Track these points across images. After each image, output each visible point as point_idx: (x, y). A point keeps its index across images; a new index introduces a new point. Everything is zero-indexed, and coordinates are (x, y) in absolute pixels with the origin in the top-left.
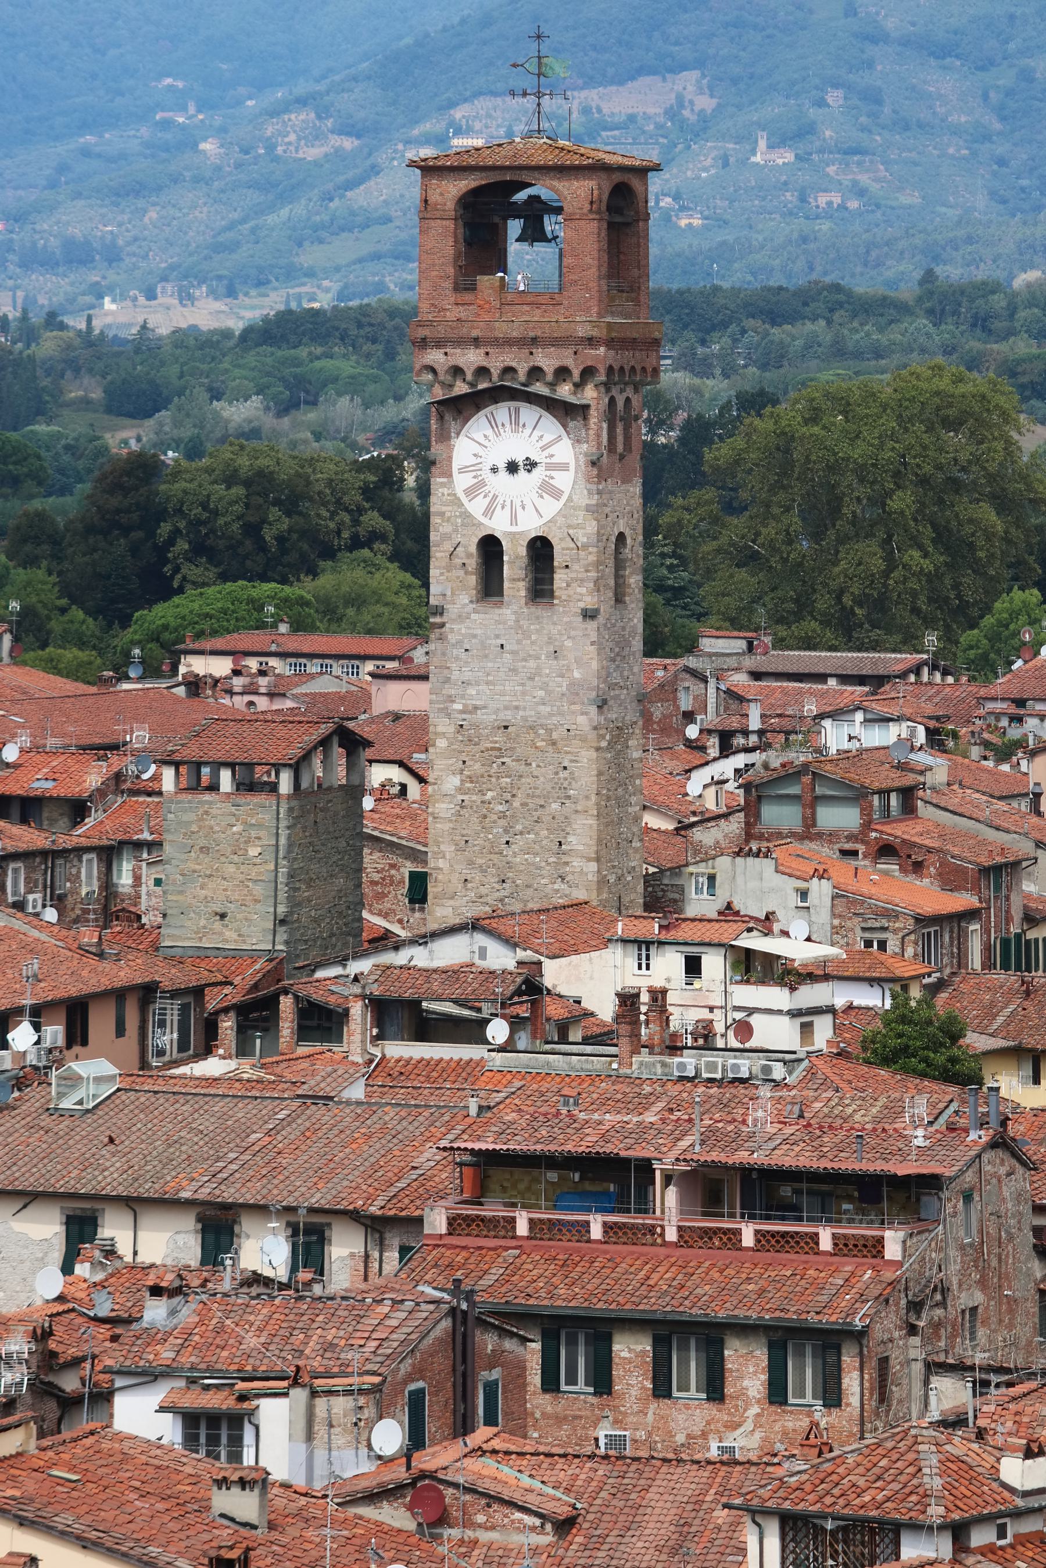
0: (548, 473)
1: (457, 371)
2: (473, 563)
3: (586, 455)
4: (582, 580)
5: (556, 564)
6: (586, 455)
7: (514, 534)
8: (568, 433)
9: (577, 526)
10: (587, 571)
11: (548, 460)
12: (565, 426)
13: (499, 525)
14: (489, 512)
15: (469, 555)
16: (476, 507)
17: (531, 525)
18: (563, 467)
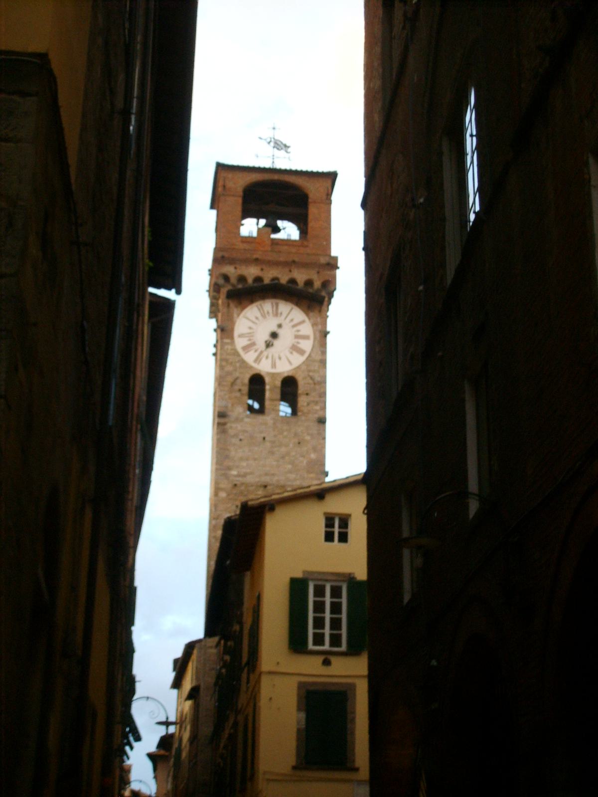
1: (242, 279)
3: (320, 332)
8: (309, 319)
9: (314, 371)
11: (296, 333)
12: (307, 315)
13: (264, 367)
14: (258, 360)
15: (243, 385)
16: (249, 357)
17: (284, 368)
18: (306, 337)
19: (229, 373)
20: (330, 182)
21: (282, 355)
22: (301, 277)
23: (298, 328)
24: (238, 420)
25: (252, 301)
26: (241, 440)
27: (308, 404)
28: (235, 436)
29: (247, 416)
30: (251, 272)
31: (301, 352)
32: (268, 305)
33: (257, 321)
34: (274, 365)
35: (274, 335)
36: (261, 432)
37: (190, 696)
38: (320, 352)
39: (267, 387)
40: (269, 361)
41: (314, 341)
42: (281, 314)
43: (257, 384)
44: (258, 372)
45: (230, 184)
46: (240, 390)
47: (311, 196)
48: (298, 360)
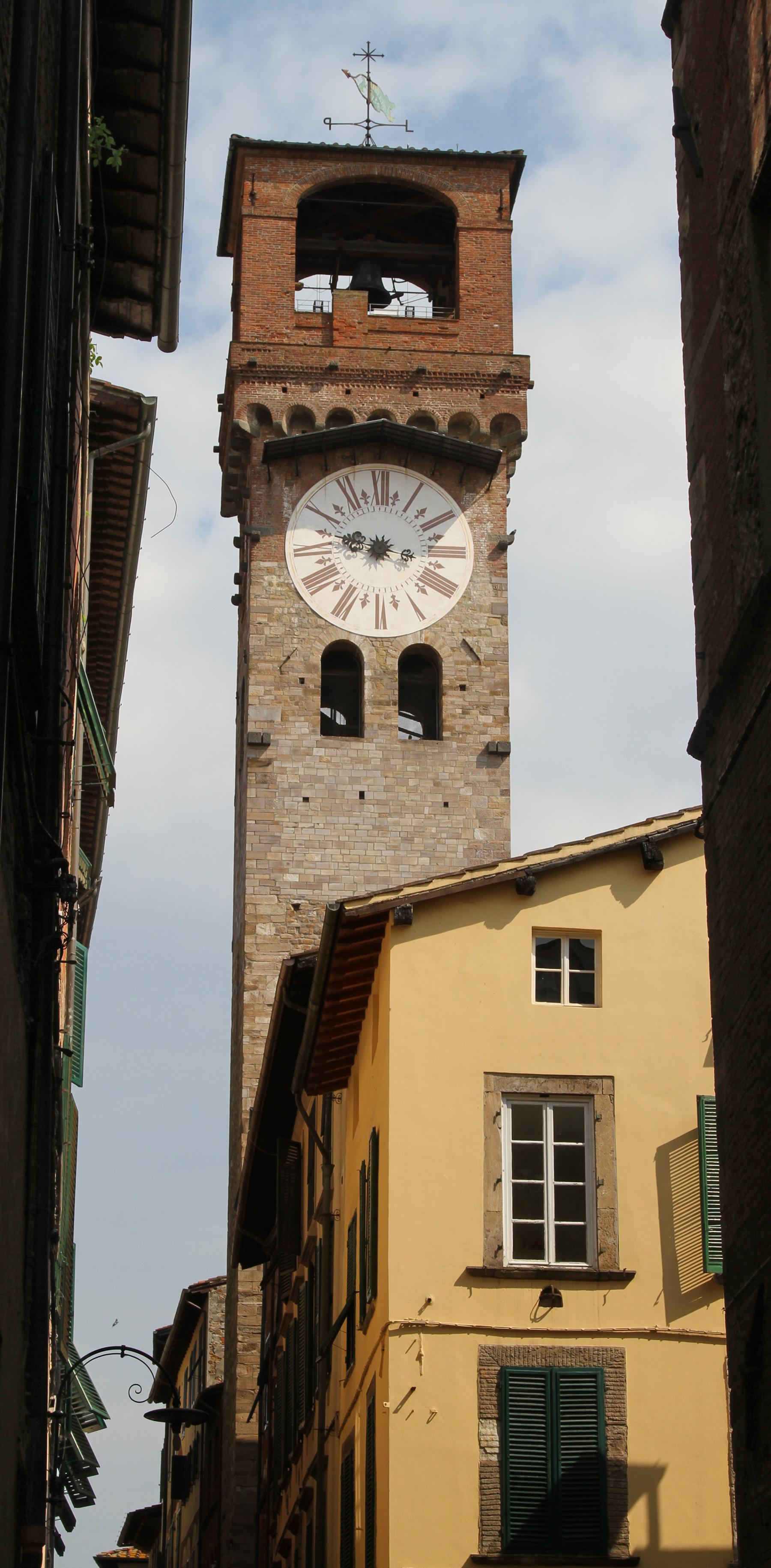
5: (445, 682)
13: (358, 626)
15: (310, 668)
16: (323, 602)
21: (400, 596)
32: (362, 478)
41: (476, 560)
42: (396, 495)
44: (344, 637)
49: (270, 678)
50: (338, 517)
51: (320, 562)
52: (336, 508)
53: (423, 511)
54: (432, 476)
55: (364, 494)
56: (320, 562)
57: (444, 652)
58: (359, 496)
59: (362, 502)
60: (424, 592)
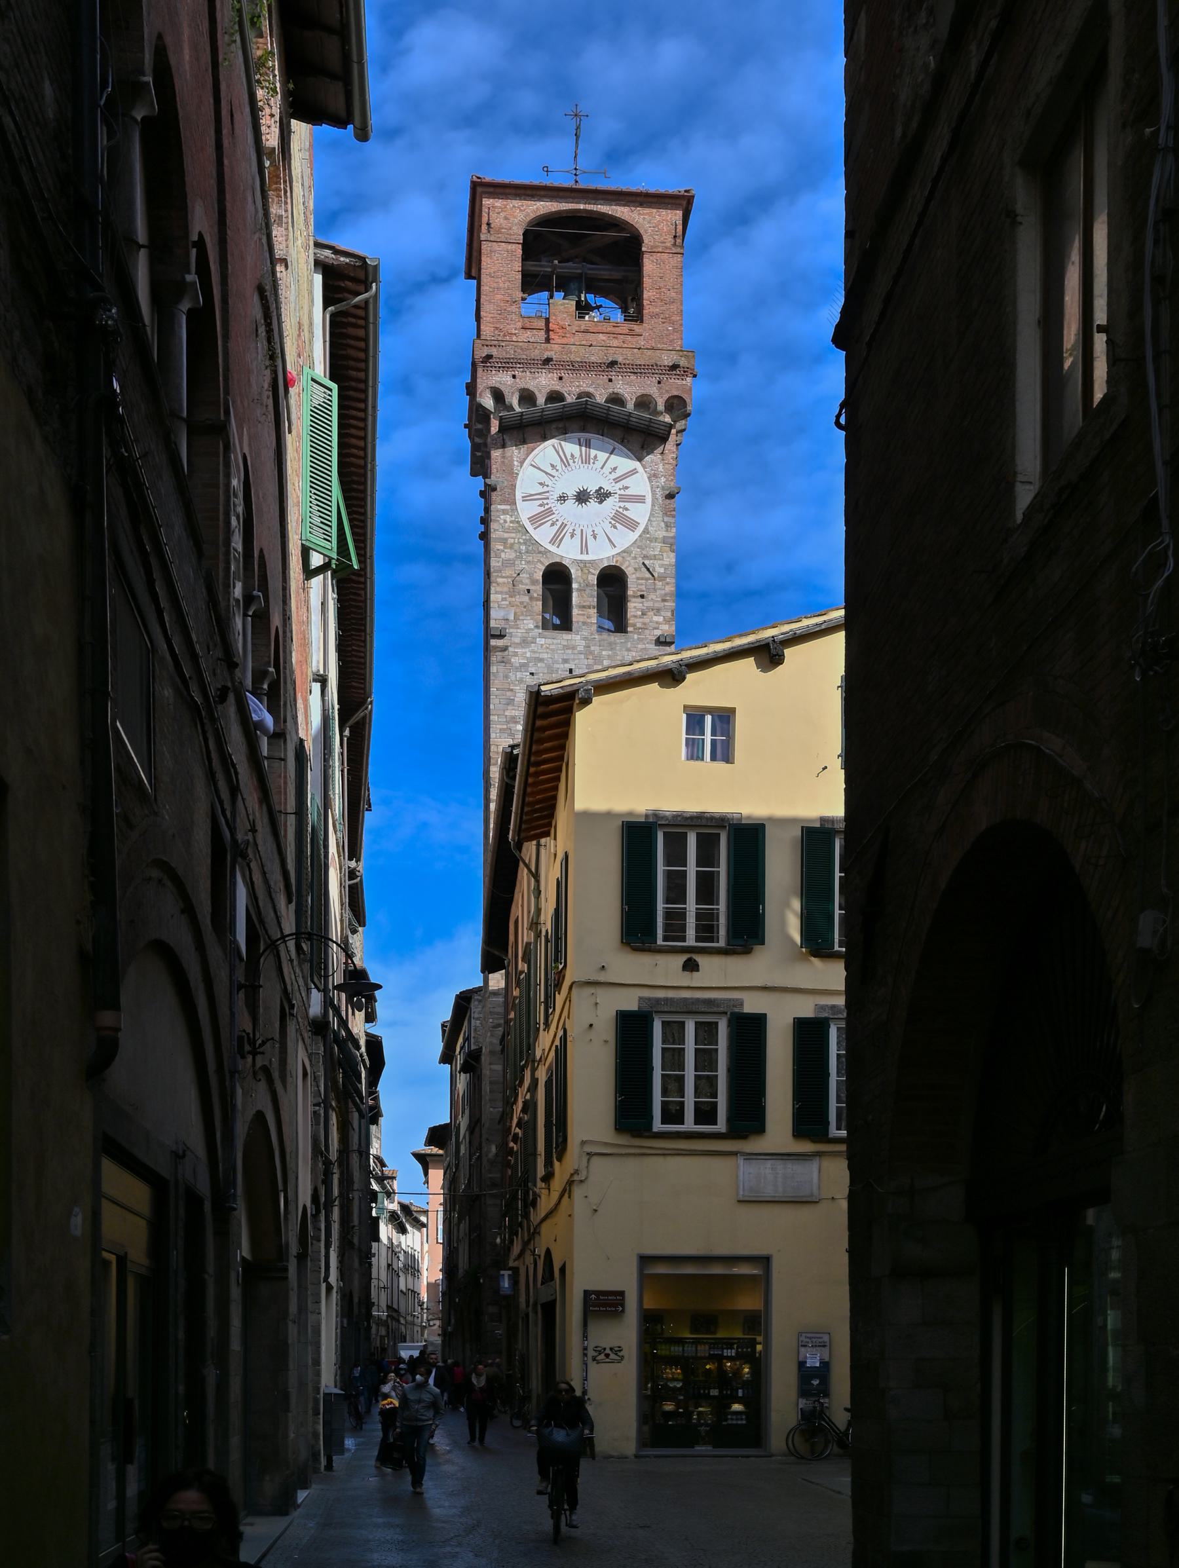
0: (622, 504)
1: (527, 397)
2: (538, 589)
3: (663, 488)
4: (658, 610)
5: (630, 593)
6: (663, 488)
7: (584, 562)
8: (644, 467)
9: (655, 557)
10: (664, 600)
11: (622, 492)
13: (568, 553)
14: (556, 540)
15: (534, 582)
16: (543, 535)
17: (603, 554)
18: (640, 499)
19: (509, 563)
20: (679, 213)
22: (629, 389)
23: (624, 483)
24: (525, 642)
25: (545, 438)
26: (532, 674)
27: (643, 614)
28: (523, 666)
29: (540, 636)
30: (542, 383)
31: (631, 525)
33: (553, 472)
34: (584, 549)
35: (582, 497)
36: (565, 661)
37: (464, 1069)
38: (663, 525)
39: (575, 586)
40: (577, 540)
41: (653, 505)
43: (557, 579)
45: (497, 220)
46: (529, 591)
47: (648, 242)
48: (626, 538)
49: (506, 589)
50: (553, 472)
51: (541, 505)
52: (552, 466)
53: (615, 469)
54: (622, 442)
55: (572, 456)
56: (541, 505)
57: (629, 571)
58: (569, 457)
59: (571, 462)
60: (615, 527)
